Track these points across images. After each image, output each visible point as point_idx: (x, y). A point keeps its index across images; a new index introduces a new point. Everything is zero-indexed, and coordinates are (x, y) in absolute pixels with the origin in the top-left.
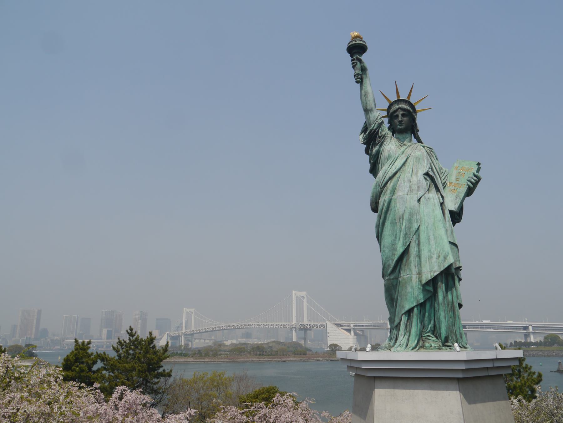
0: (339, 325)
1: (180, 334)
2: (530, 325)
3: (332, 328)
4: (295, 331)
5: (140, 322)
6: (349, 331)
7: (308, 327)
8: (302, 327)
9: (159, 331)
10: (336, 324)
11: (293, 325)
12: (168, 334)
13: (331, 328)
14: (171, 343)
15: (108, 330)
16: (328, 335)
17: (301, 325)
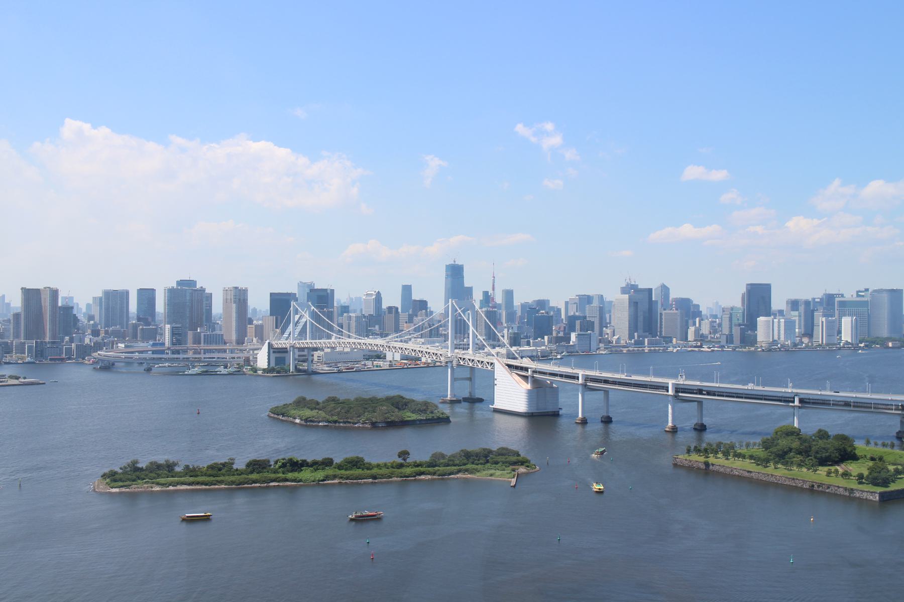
0: (510, 366)
1: (288, 346)
2: (797, 394)
3: (501, 373)
4: (452, 367)
5: (234, 306)
6: (525, 378)
7: (471, 365)
8: (462, 363)
9: (274, 317)
10: (510, 366)
11: (449, 357)
12: (269, 343)
13: (501, 374)
14: (276, 358)
15: (173, 327)
16: (496, 382)
17: (461, 358)
